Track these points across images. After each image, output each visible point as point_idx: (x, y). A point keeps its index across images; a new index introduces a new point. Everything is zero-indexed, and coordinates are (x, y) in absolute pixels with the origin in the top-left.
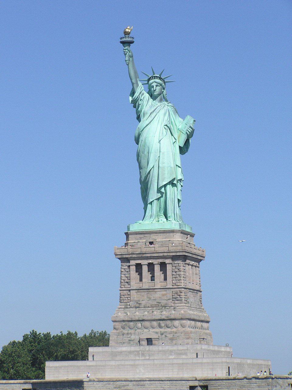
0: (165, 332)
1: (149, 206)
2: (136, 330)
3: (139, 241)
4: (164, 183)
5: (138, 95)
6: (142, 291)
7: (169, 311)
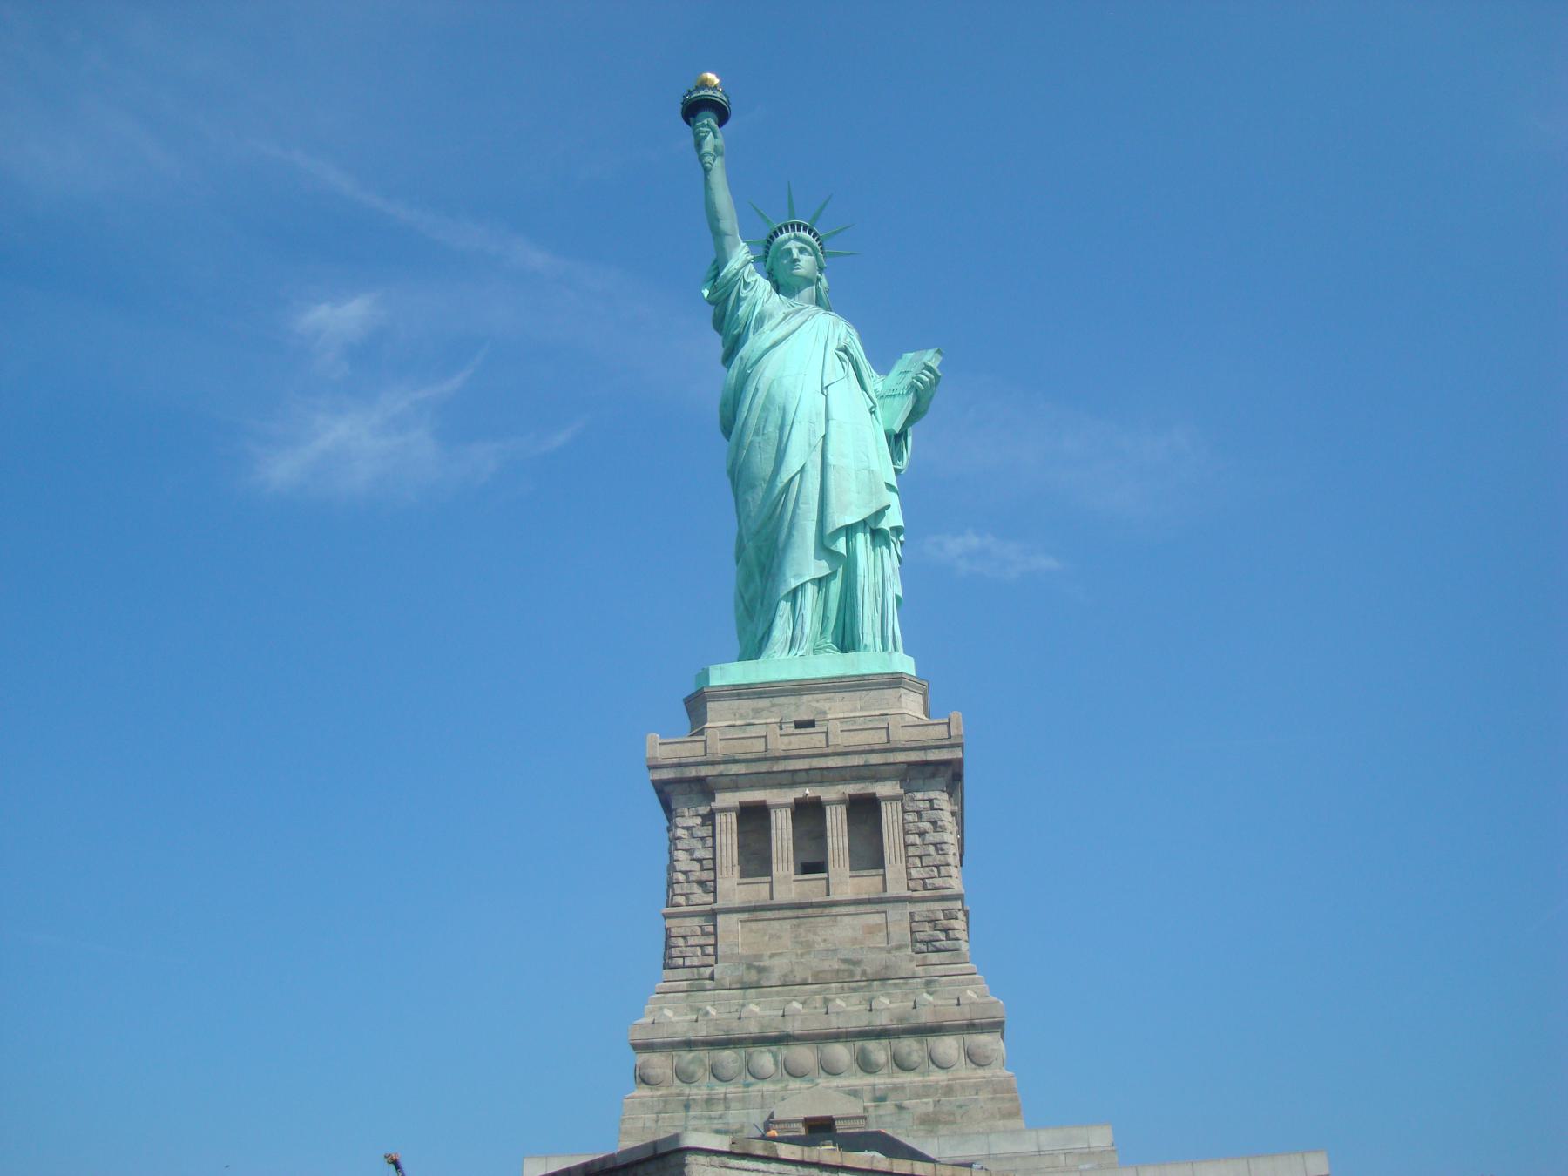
0: (896, 1088)
1: (784, 608)
2: (748, 1085)
3: (752, 721)
4: (850, 519)
5: (737, 266)
6: (769, 914)
7: (906, 994)
